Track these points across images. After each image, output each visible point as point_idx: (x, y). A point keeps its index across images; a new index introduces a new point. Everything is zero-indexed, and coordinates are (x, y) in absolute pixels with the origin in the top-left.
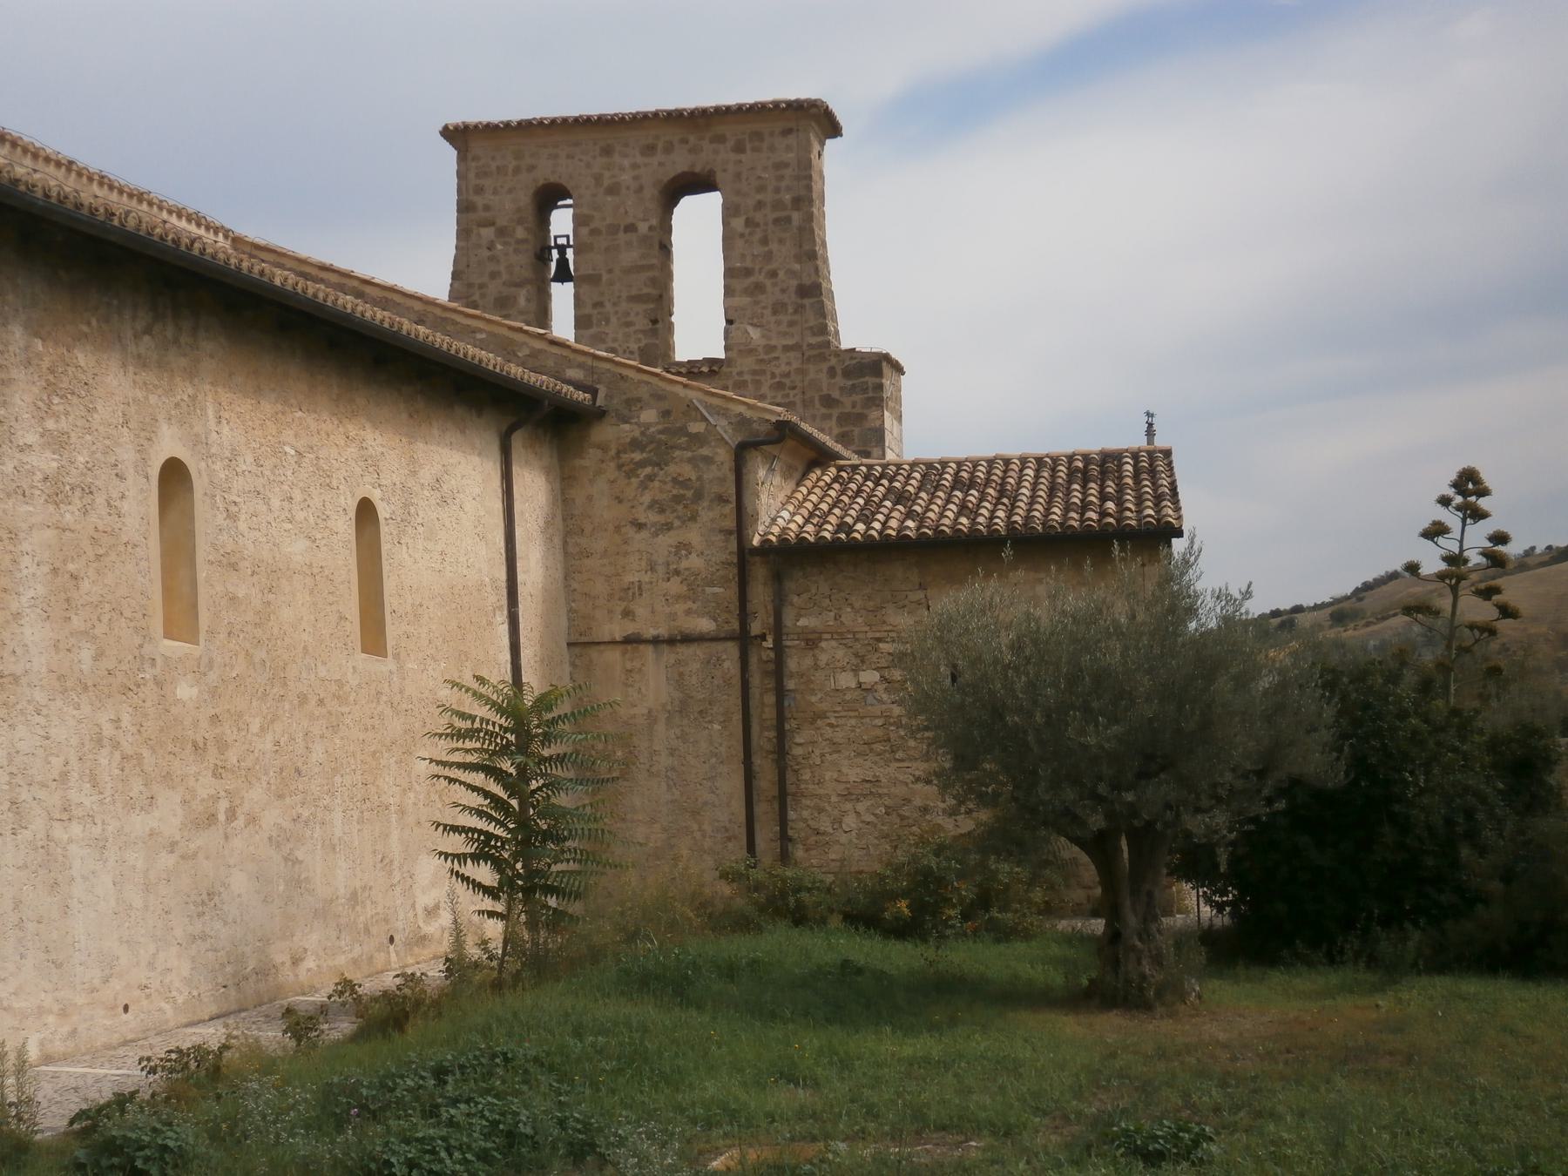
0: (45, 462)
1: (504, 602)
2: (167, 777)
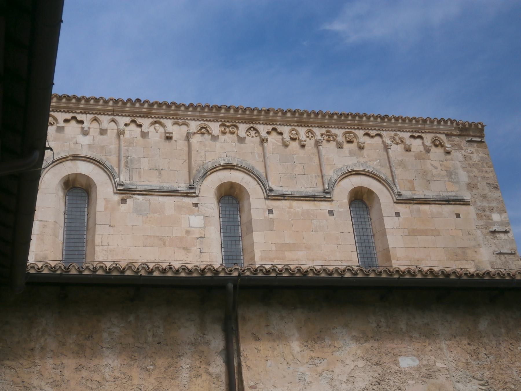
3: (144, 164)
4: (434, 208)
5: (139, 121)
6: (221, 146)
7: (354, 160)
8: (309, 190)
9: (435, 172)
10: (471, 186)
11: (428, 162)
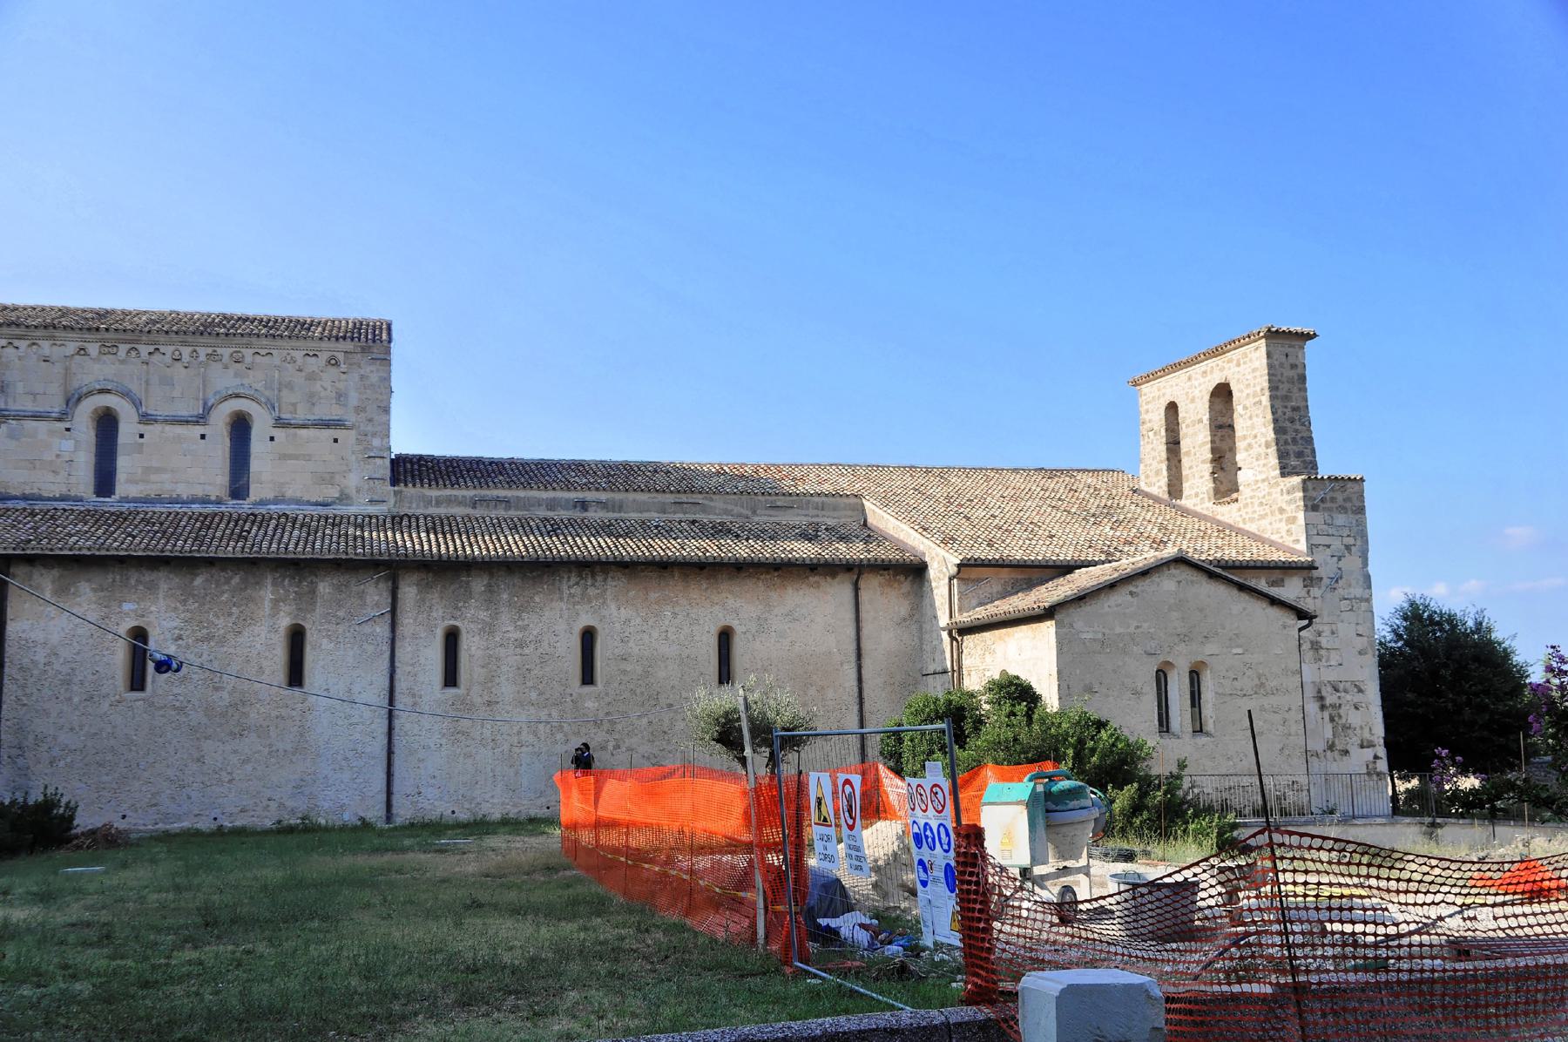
0: (518, 635)
1: (853, 658)
3: (20, 388)
4: (311, 432)
5: (16, 343)
6: (97, 369)
7: (238, 381)
8: (184, 411)
9: (323, 394)
10: (359, 410)
11: (319, 383)
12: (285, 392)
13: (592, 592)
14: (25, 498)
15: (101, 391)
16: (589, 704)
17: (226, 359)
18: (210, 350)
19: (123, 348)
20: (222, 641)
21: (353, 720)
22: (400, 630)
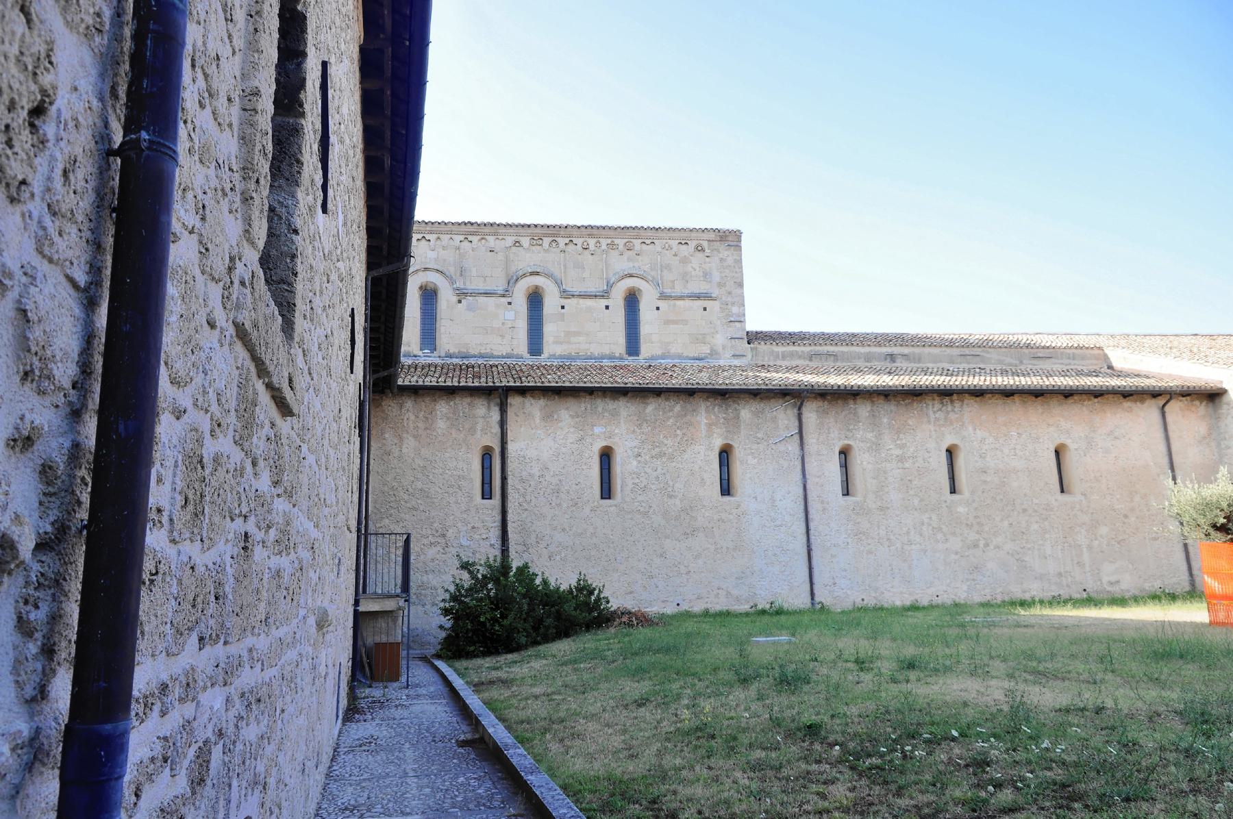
0: (899, 452)
2: (954, 534)
3: (474, 273)
5: (470, 238)
6: (528, 258)
7: (631, 265)
8: (592, 288)
10: (720, 285)
12: (665, 272)
13: (952, 416)
14: (481, 356)
15: (532, 274)
16: (961, 509)
17: (621, 247)
18: (609, 241)
19: (547, 241)
20: (671, 458)
21: (778, 523)
22: (806, 448)
